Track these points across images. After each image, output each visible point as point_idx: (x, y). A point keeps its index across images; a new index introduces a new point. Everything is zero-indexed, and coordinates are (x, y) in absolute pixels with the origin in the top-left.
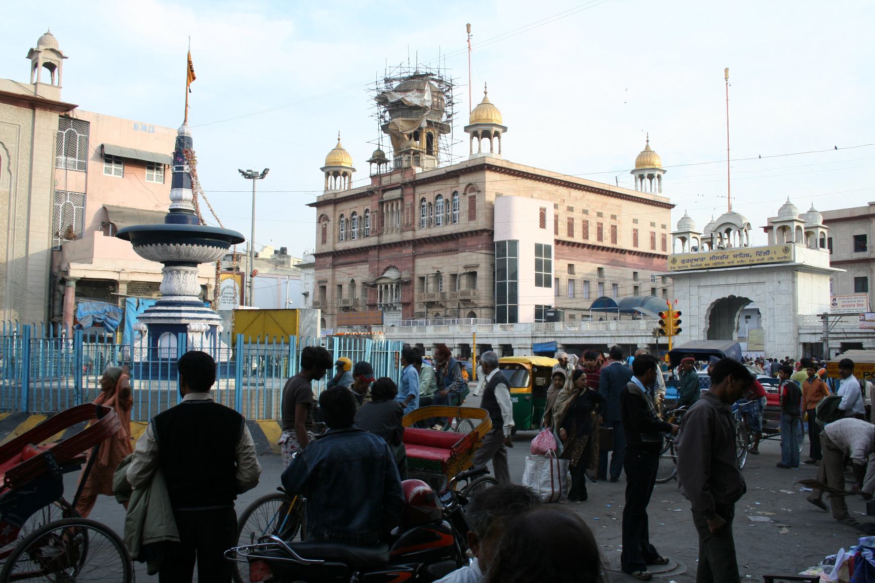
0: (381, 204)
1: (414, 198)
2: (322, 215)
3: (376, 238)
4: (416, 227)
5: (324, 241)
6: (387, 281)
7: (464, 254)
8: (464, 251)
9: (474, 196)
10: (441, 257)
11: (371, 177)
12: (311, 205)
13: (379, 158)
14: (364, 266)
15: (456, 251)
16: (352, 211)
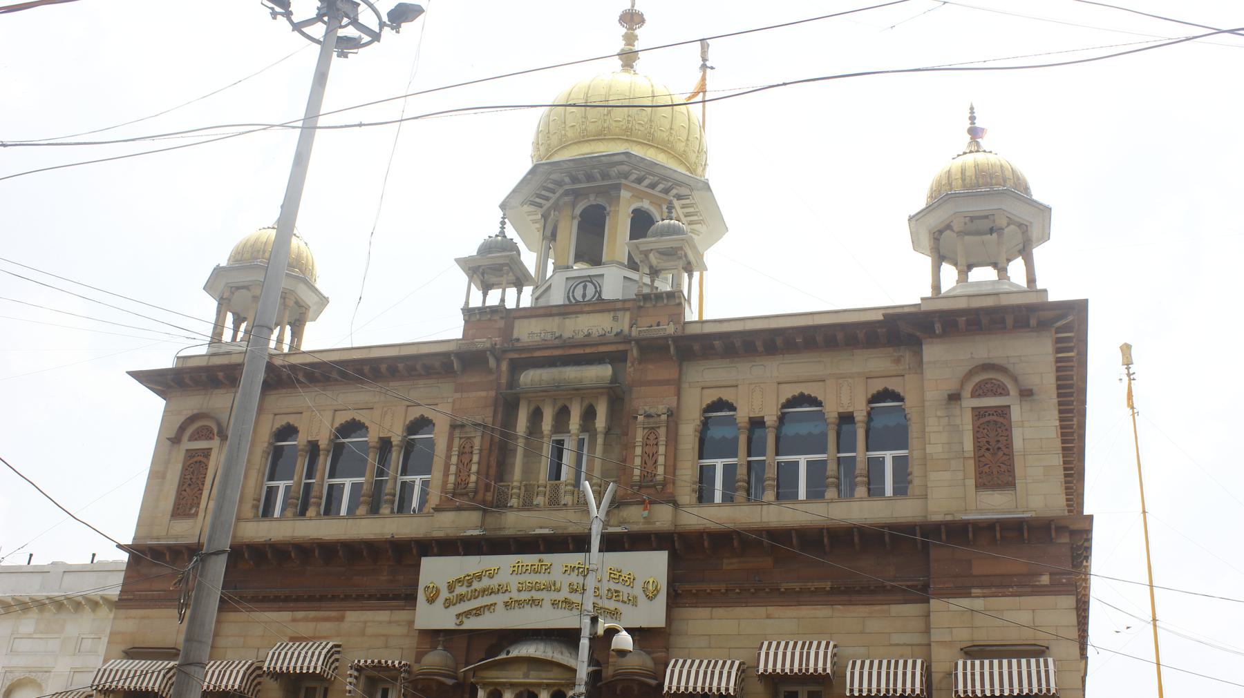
0: (508, 405)
1: (678, 395)
2: (192, 419)
3: (474, 517)
4: (686, 495)
5: (184, 506)
6: (534, 677)
7: (965, 602)
8: (963, 591)
9: (1004, 411)
10: (822, 612)
11: (468, 312)
12: (153, 380)
13: (492, 265)
14: (383, 616)
15: (921, 593)
16: (343, 418)
